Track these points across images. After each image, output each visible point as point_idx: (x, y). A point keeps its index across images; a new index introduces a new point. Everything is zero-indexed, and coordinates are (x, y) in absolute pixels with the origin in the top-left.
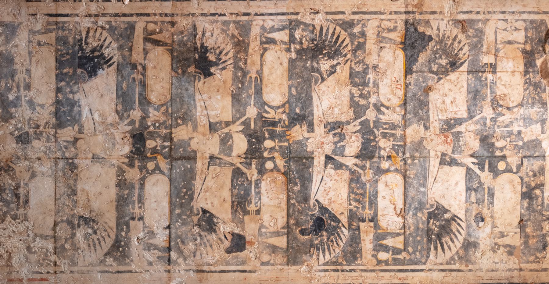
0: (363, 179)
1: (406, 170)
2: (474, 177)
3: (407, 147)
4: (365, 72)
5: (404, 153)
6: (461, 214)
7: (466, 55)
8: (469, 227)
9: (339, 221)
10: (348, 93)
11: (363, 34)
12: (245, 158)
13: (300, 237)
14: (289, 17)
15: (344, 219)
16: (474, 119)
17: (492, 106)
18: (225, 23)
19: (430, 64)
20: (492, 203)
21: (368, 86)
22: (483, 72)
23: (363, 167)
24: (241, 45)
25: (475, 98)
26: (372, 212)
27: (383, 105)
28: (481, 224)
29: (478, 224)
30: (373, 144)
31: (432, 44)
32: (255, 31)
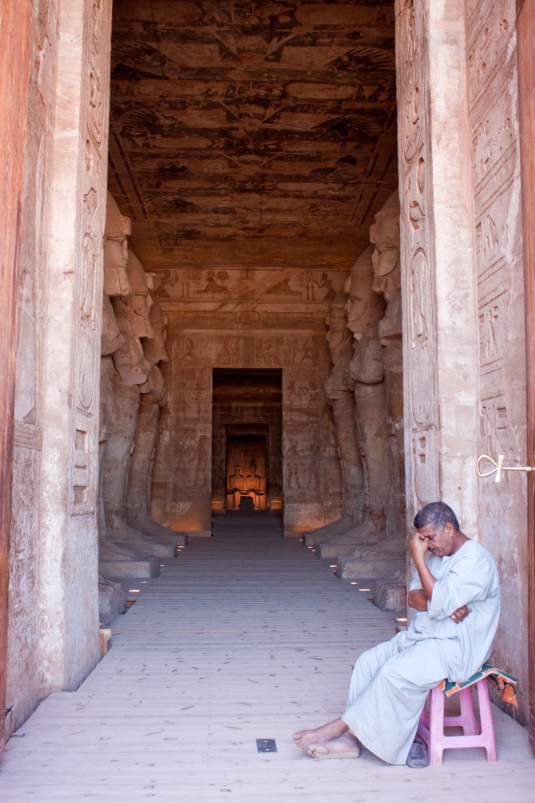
0: (291, 104)
1: (284, 81)
2: (297, 40)
3: (258, 80)
4: (170, 102)
5: (265, 82)
6: (344, 50)
7: (137, 43)
8: (364, 44)
9: (337, 119)
10: (195, 111)
11: (126, 103)
12: (264, 156)
13: (348, 136)
14: (119, 136)
15: (334, 117)
16: (220, 39)
17: (202, 26)
18: (133, 161)
19: (152, 66)
20: (335, 26)
21: (186, 101)
22: (156, 31)
23: (278, 106)
24: (152, 156)
25: (194, 39)
26: (331, 102)
27: (207, 92)
28: (361, 35)
29: (361, 37)
30: (252, 99)
31: (127, 64)
32: (137, 150)
